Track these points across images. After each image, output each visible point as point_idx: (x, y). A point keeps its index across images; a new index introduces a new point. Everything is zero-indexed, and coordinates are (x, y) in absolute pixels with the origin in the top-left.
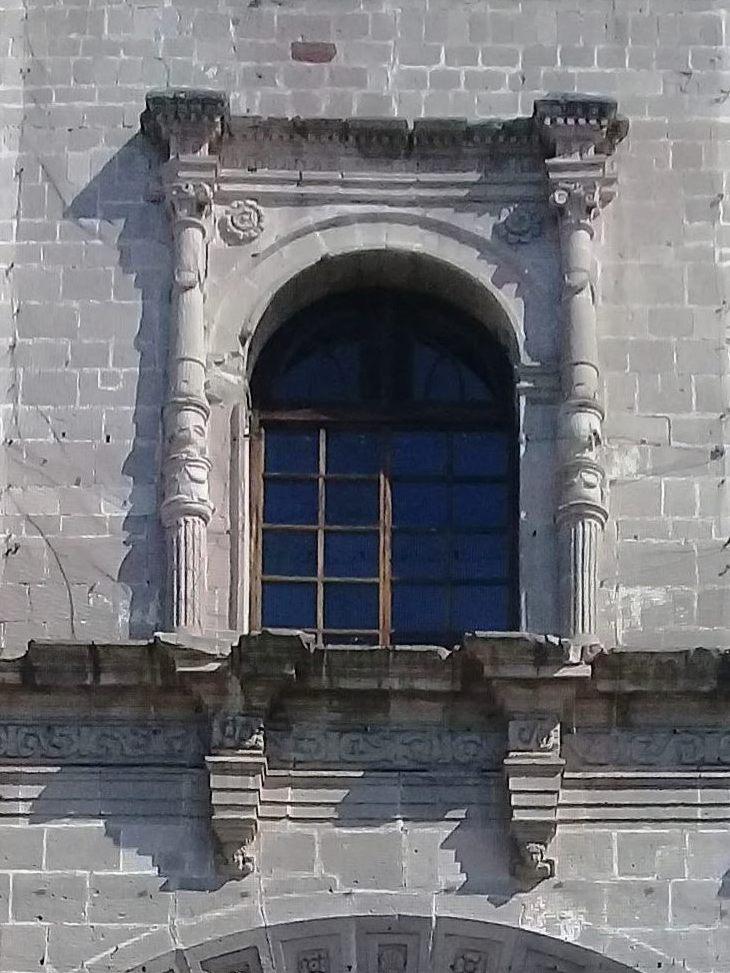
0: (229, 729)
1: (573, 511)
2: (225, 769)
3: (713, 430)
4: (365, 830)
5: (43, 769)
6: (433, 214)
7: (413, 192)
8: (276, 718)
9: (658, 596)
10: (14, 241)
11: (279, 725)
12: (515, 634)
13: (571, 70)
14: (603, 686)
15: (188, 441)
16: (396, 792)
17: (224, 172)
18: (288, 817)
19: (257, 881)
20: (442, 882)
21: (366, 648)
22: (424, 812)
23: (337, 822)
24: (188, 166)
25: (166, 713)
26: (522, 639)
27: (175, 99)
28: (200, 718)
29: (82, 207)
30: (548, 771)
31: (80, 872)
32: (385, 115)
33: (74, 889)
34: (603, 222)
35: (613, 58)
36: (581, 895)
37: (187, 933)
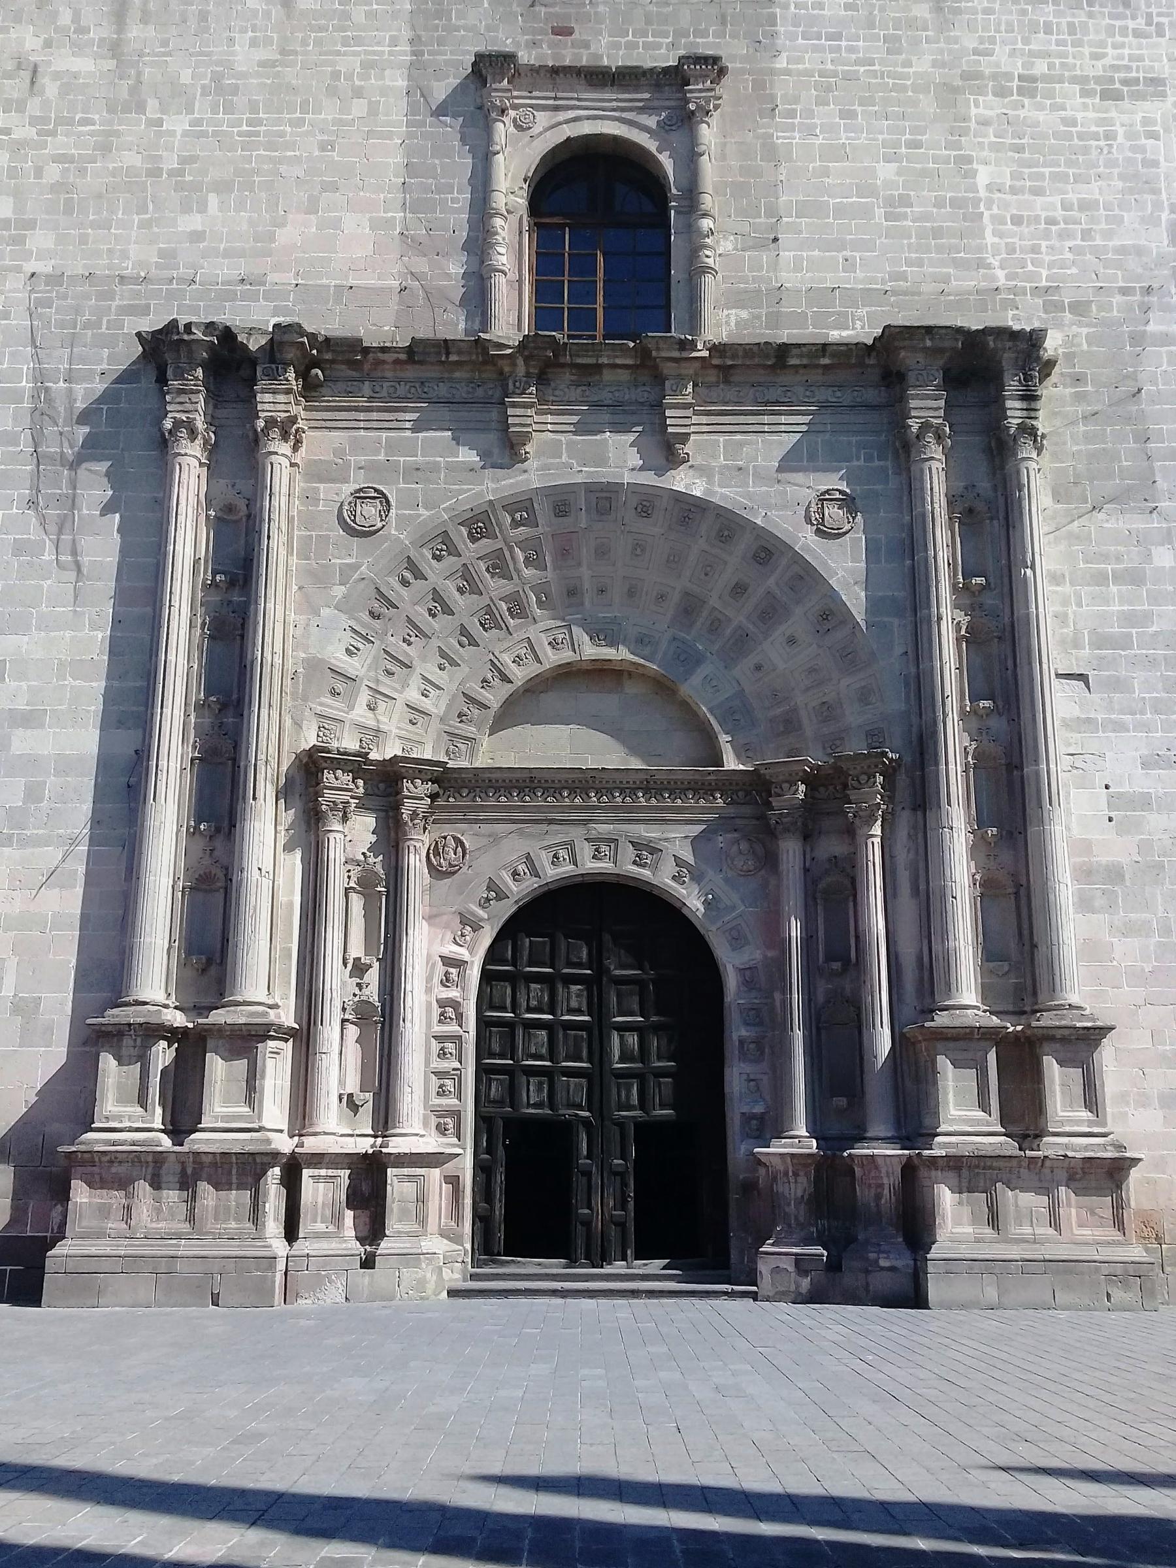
0: (518, 384)
1: (701, 269)
2: (514, 405)
3: (773, 227)
4: (590, 437)
6: (624, 115)
7: (615, 104)
8: (542, 379)
9: (744, 314)
10: (404, 129)
11: (545, 382)
12: (669, 334)
13: (698, 40)
14: (715, 362)
15: (497, 233)
16: (607, 417)
17: (515, 93)
18: (548, 431)
19: (532, 464)
20: (630, 464)
21: (590, 342)
23: (575, 433)
24: (496, 90)
27: (490, 56)
28: (502, 378)
29: (441, 111)
30: (686, 406)
32: (600, 64)
33: (434, 468)
34: (715, 119)
35: (721, 34)
36: (703, 471)
37: (495, 491)
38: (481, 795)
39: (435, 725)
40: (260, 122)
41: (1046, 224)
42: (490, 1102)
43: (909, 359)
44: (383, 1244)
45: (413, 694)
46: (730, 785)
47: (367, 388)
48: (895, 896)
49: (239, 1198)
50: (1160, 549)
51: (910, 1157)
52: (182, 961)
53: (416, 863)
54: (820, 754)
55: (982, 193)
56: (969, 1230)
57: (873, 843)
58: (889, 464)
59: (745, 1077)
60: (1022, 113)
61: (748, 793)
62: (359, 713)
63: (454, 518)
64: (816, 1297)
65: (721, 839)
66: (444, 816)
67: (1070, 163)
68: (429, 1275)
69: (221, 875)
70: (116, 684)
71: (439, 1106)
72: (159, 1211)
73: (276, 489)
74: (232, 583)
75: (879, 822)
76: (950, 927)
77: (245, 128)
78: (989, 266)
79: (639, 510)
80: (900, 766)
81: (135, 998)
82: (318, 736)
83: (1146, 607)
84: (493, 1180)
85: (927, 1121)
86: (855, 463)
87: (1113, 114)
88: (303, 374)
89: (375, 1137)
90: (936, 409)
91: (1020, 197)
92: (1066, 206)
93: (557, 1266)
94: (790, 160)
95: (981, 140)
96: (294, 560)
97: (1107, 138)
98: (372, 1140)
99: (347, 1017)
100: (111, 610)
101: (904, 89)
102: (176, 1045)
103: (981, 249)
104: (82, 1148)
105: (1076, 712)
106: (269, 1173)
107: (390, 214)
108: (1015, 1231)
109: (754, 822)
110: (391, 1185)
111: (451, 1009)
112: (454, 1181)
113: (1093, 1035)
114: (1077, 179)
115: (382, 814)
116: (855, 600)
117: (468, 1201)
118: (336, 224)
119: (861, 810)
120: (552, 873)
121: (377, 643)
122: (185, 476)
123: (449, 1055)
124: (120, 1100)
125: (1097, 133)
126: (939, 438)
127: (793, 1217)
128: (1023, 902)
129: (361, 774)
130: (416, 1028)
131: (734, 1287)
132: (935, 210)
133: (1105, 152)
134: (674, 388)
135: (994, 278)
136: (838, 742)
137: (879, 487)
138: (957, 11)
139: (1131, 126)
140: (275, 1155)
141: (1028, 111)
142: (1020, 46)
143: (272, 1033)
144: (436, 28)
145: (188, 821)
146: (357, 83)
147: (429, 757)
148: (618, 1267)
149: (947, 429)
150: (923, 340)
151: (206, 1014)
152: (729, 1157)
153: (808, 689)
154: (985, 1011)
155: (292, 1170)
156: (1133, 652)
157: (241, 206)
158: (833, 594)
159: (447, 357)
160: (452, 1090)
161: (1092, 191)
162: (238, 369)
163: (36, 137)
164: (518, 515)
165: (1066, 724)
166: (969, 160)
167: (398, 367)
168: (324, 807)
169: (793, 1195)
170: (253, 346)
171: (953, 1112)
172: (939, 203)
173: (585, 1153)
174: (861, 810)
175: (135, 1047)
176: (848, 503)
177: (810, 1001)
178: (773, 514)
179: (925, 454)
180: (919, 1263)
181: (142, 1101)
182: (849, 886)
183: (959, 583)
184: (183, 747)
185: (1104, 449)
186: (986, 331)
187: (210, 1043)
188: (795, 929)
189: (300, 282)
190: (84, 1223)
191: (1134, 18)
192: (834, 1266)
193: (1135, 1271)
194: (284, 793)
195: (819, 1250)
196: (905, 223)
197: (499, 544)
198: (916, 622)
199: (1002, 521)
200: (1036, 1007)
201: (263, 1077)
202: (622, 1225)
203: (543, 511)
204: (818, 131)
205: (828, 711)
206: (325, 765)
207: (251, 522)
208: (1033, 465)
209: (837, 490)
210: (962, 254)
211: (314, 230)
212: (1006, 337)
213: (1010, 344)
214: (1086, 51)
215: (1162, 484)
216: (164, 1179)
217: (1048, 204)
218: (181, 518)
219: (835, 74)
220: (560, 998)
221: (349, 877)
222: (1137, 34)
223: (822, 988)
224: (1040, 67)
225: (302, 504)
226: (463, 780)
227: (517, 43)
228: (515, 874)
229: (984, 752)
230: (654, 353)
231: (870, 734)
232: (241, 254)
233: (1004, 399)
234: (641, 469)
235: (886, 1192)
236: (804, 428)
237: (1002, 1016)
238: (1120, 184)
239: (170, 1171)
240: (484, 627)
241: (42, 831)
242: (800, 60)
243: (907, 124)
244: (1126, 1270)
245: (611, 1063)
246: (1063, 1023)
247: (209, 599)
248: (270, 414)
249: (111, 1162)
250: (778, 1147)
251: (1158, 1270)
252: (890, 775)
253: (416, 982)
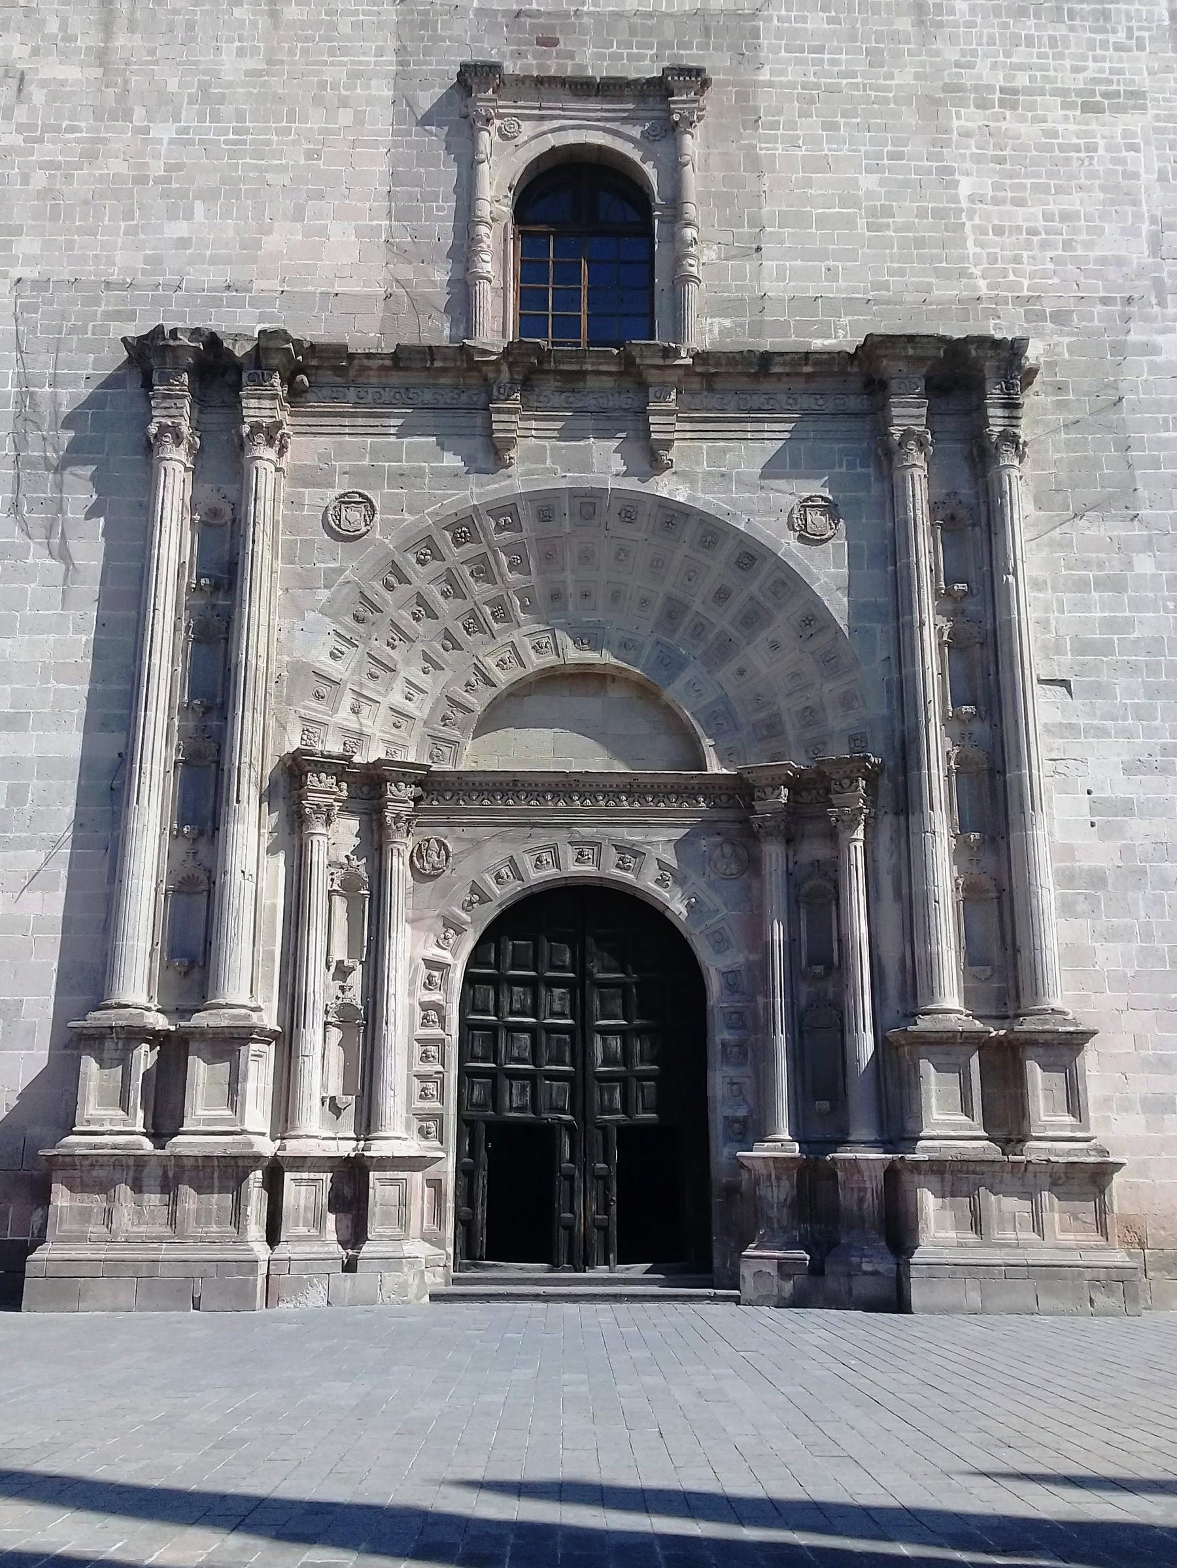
0: (502, 390)
1: (683, 278)
2: (499, 411)
3: (757, 237)
4: (573, 443)
5: (404, 411)
6: (609, 125)
7: (599, 114)
8: (527, 384)
9: (727, 323)
10: (390, 138)
12: (652, 342)
13: (681, 52)
14: (699, 369)
15: (482, 241)
17: (500, 103)
20: (614, 470)
21: (574, 348)
22: (604, 434)
23: (558, 439)
24: (482, 100)
25: (469, 381)
26: (657, 345)
27: (475, 66)
28: (487, 385)
29: (426, 120)
30: (670, 413)
31: (423, 464)
32: (585, 74)
33: (419, 473)
34: (698, 130)
35: (706, 47)
36: (686, 477)
38: (465, 798)
39: (419, 729)
40: (246, 131)
41: (1027, 234)
42: (472, 1105)
43: (891, 367)
44: (365, 1248)
45: (396, 698)
46: (712, 788)
47: (352, 394)
48: (878, 899)
49: (221, 1201)
50: (1142, 556)
51: (893, 1161)
52: (165, 964)
53: (399, 866)
54: (803, 759)
55: (964, 204)
56: (952, 1234)
57: (855, 847)
58: (871, 470)
59: (728, 1080)
60: (1004, 125)
61: (730, 797)
62: (344, 716)
63: (438, 523)
64: (799, 1301)
65: (704, 842)
66: (425, 819)
67: (1051, 175)
68: (411, 1279)
69: (203, 877)
70: (99, 686)
71: (421, 1109)
72: (140, 1214)
73: (261, 493)
74: (216, 587)
75: (861, 827)
76: (933, 931)
77: (231, 136)
78: (971, 276)
79: (623, 515)
80: (882, 770)
81: (117, 1001)
82: (302, 739)
83: (1127, 614)
84: (475, 1187)
85: (910, 1125)
86: (837, 470)
87: (1094, 126)
88: (289, 380)
89: (358, 1140)
90: (918, 417)
91: (1002, 207)
92: (1047, 217)
93: (540, 1270)
94: (773, 170)
95: (962, 151)
96: (279, 565)
97: (1088, 149)
98: (355, 1143)
99: (329, 1020)
100: (95, 614)
101: (886, 101)
102: (158, 1048)
103: (964, 258)
104: (63, 1151)
105: (1059, 718)
106: (251, 1176)
107: (375, 222)
108: (997, 1235)
109: (737, 826)
110: (373, 1188)
111: (433, 1012)
112: (436, 1185)
113: (1075, 1039)
114: (1059, 190)
115: (365, 817)
116: (838, 606)
117: (450, 1205)
118: (323, 231)
119: (844, 814)
120: (535, 876)
121: (361, 646)
122: (170, 480)
123: (431, 1059)
124: (102, 1103)
125: (1079, 144)
126: (921, 445)
127: (775, 1220)
128: (1006, 907)
129: (345, 777)
130: (399, 1031)
131: (717, 1291)
132: (917, 220)
133: (1086, 163)
134: (658, 395)
135: (975, 288)
136: (821, 747)
137: (861, 494)
138: (940, 25)
139: (1112, 137)
140: (257, 1158)
141: (1009, 123)
142: (1001, 58)
143: (254, 1036)
144: (422, 39)
145: (171, 824)
146: (344, 92)
147: (413, 760)
148: (601, 1271)
149: (929, 437)
150: (905, 348)
151: (188, 1017)
152: (712, 1160)
153: (790, 694)
154: (967, 1015)
155: (274, 1173)
156: (1114, 658)
157: (226, 214)
158: (816, 600)
159: (432, 363)
160: (435, 1093)
161: (1074, 202)
162: (223, 375)
163: (23, 144)
164: (502, 520)
165: (1048, 729)
166: (949, 171)
167: (383, 373)
168: (307, 810)
169: (776, 1200)
170: (239, 352)
171: (936, 1116)
172: (922, 213)
173: (568, 1156)
174: (844, 814)
175: (116, 1050)
176: (831, 509)
177: (792, 1003)
178: (757, 520)
179: (907, 460)
180: (902, 1268)
181: (124, 1104)
182: (833, 891)
183: (942, 589)
184: (166, 750)
185: (1085, 457)
186: (968, 340)
187: (193, 1046)
188: (778, 933)
189: (286, 289)
190: (65, 1227)
191: (1114, 31)
192: (816, 1270)
193: (1117, 1277)
194: (268, 796)
195: (803, 1254)
196: (887, 233)
197: (485, 549)
198: (898, 629)
199: (984, 528)
200: (1019, 1012)
201: (245, 1080)
202: (604, 1229)
203: (527, 514)
204: (801, 142)
205: (810, 716)
206: (308, 768)
207: (236, 525)
208: (1015, 473)
209: (820, 497)
210: (944, 264)
211: (300, 237)
212: (988, 345)
213: (990, 353)
214: (1068, 63)
215: (1143, 492)
216: (146, 1182)
217: (1031, 214)
218: (166, 522)
219: (817, 86)
220: (543, 1002)
221: (332, 880)
222: (1118, 48)
223: (804, 990)
224: (1022, 80)
225: (287, 509)
226: (447, 783)
227: (501, 54)
228: (498, 877)
229: (967, 757)
230: (638, 361)
231: (852, 739)
232: (228, 261)
233: (985, 407)
234: (625, 474)
235: (869, 1195)
236: (787, 435)
237: (985, 1022)
238: (1101, 196)
239: (152, 1174)
240: (468, 631)
241: (24, 834)
242: (783, 72)
243: (889, 135)
244: (1108, 1274)
245: (593, 1065)
246: (1046, 1027)
247: (193, 602)
248: (255, 419)
249: (92, 1165)
250: (760, 1151)
251: (1141, 1275)
252: (872, 778)
253: (398, 985)
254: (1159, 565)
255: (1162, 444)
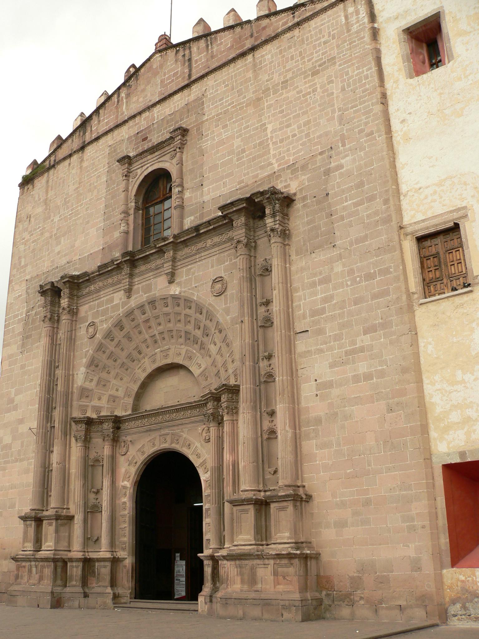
3: (201, 180)
9: (192, 218)
36: (179, 284)
67: (300, 109)
78: (272, 164)
86: (226, 264)
135: (274, 168)
210: (263, 164)
214: (306, 60)
222: (325, 43)
254: (344, 266)
255: (345, 208)
